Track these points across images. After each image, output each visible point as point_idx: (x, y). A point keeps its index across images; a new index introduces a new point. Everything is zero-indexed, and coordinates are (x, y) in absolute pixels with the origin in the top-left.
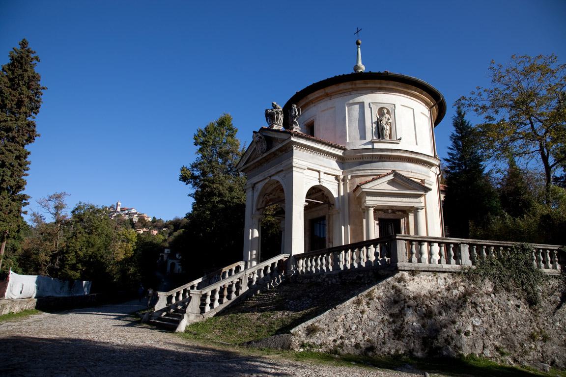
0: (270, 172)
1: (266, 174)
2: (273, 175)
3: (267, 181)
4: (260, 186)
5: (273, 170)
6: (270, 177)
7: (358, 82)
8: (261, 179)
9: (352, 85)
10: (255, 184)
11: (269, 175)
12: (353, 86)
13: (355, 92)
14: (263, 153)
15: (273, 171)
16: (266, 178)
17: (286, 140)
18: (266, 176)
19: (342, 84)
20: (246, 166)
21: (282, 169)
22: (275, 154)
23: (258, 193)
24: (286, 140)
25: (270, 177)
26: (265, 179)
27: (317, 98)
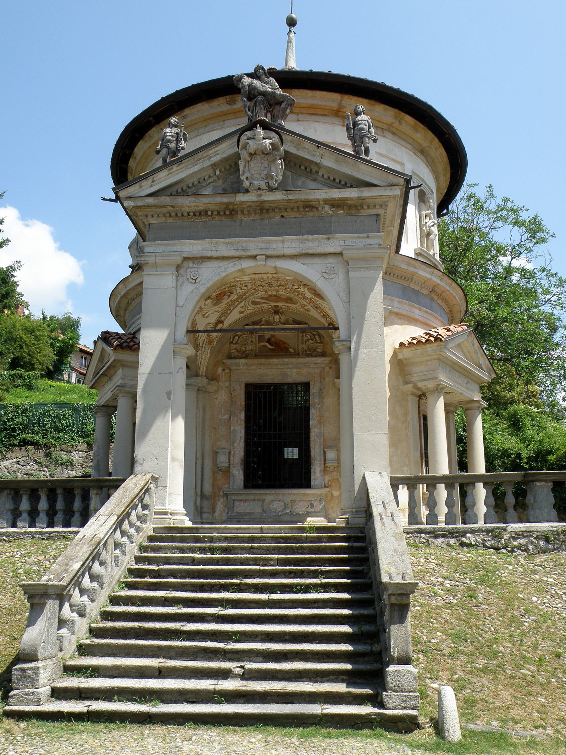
0: (274, 245)
1: (254, 245)
2: (284, 256)
3: (246, 264)
4: (210, 275)
5: (294, 244)
6: (268, 257)
7: (408, 118)
8: (225, 254)
9: (396, 118)
10: (185, 259)
11: (269, 253)
12: (396, 124)
13: (390, 135)
14: (272, 190)
15: (289, 244)
16: (254, 257)
17: (376, 186)
18: (253, 253)
19: (382, 106)
20: (165, 200)
21: (339, 250)
22: (309, 206)
23: (202, 290)
24: (376, 186)
25: (268, 257)
26: (239, 258)
27: (311, 107)
